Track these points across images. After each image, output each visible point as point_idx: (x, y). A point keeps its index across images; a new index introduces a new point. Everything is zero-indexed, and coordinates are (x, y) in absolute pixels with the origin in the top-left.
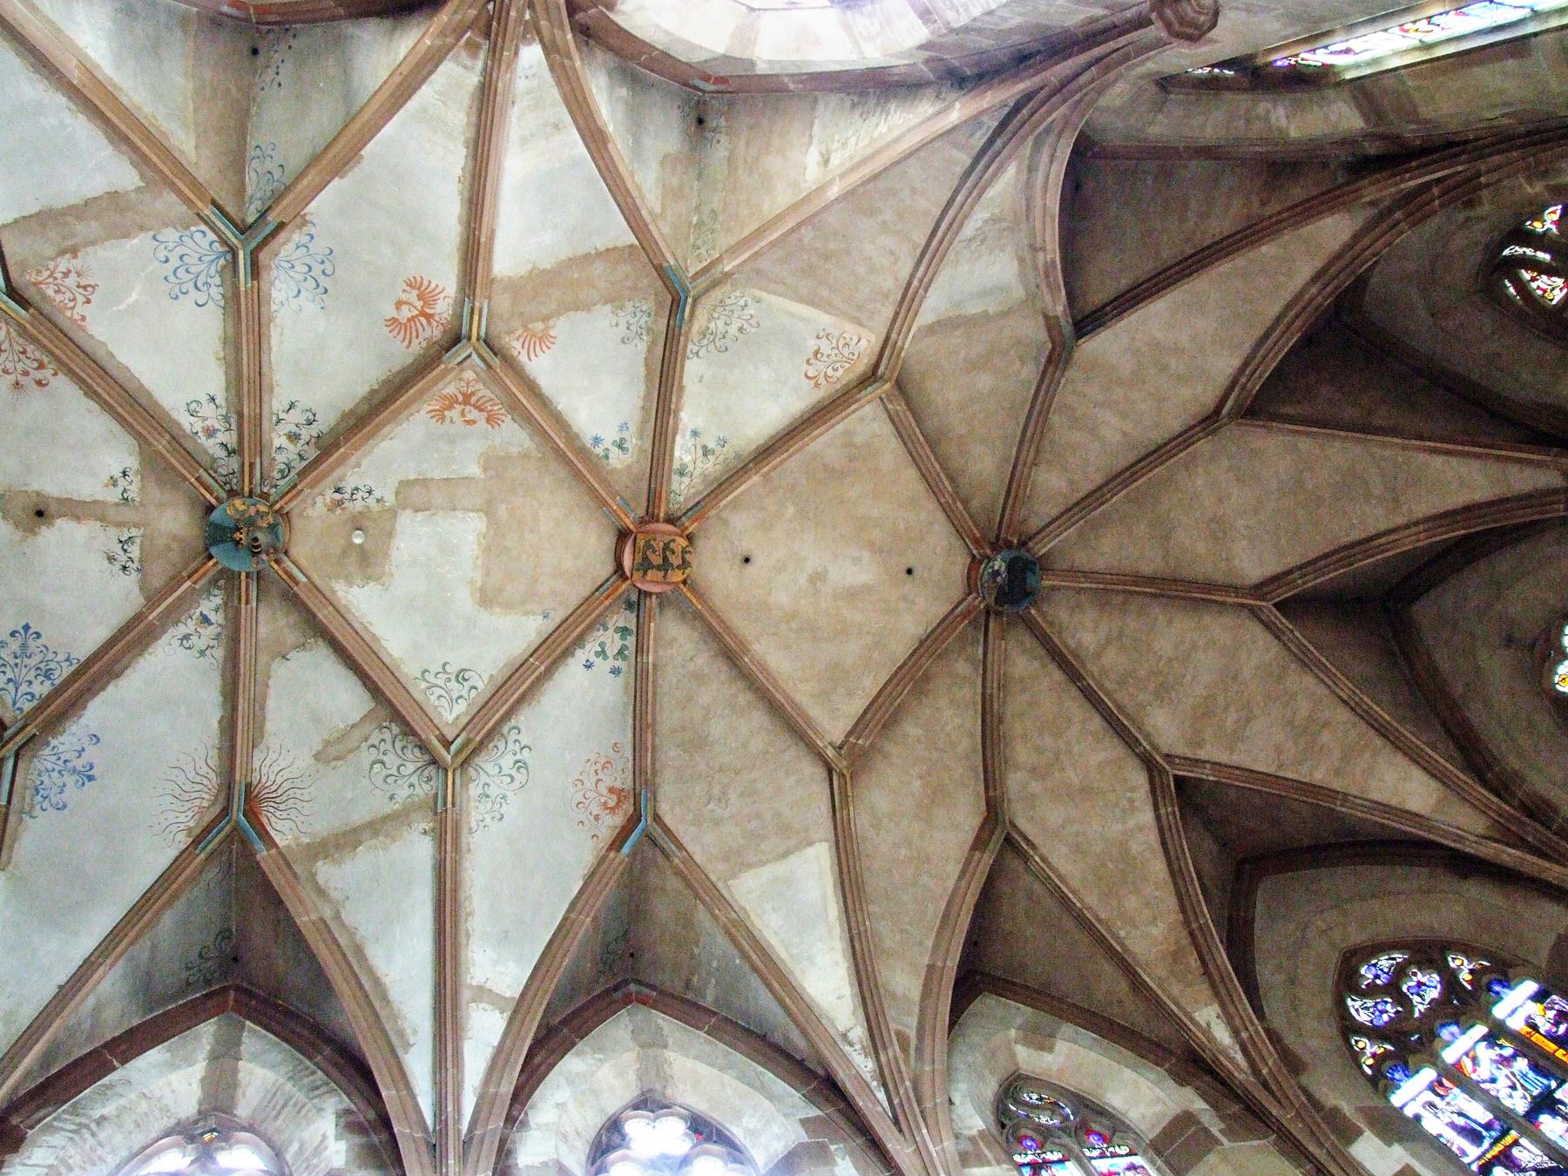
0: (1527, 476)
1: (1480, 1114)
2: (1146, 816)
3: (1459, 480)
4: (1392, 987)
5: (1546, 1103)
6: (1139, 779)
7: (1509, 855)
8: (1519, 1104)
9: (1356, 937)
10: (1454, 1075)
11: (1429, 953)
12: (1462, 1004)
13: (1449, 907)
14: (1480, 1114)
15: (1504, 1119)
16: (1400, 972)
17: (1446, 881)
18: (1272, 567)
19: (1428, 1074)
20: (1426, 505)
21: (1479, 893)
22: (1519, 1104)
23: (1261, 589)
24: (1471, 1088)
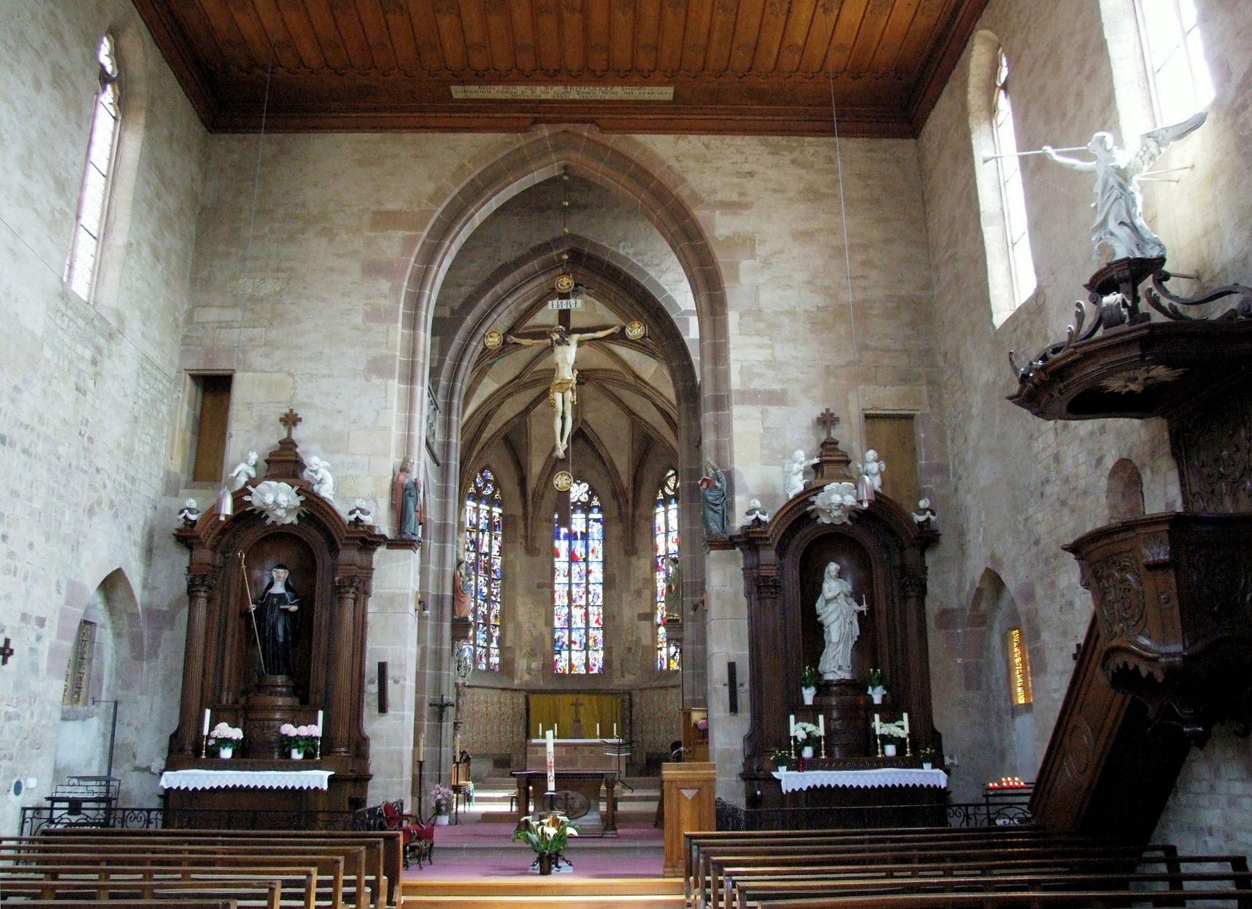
0: (626, 480)
1: (474, 521)
2: (512, 415)
3: (623, 464)
4: (486, 481)
5: (483, 531)
6: (522, 408)
7: (530, 498)
8: (481, 527)
9: (494, 466)
10: (477, 510)
11: (497, 484)
12: (491, 501)
13: (511, 485)
14: (474, 521)
15: (476, 526)
16: (489, 481)
17: (516, 480)
18: (590, 422)
19: (475, 505)
20: (614, 456)
21: (517, 491)
22: (481, 527)
23: (584, 421)
24: (478, 518)
